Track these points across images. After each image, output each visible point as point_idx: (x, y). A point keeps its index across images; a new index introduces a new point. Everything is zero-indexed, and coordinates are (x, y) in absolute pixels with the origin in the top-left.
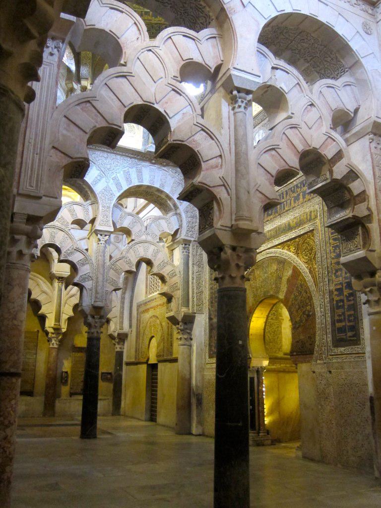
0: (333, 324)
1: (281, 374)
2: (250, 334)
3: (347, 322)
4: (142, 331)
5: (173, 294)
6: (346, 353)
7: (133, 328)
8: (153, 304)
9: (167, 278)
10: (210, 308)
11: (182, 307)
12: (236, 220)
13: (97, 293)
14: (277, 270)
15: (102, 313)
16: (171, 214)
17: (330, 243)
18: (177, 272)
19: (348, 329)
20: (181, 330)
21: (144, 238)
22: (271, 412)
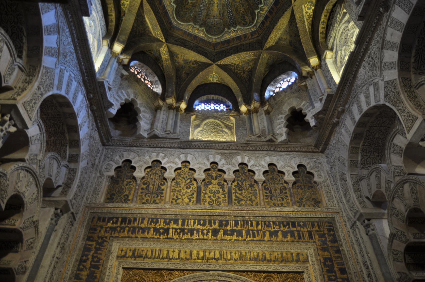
21: (35, 167)
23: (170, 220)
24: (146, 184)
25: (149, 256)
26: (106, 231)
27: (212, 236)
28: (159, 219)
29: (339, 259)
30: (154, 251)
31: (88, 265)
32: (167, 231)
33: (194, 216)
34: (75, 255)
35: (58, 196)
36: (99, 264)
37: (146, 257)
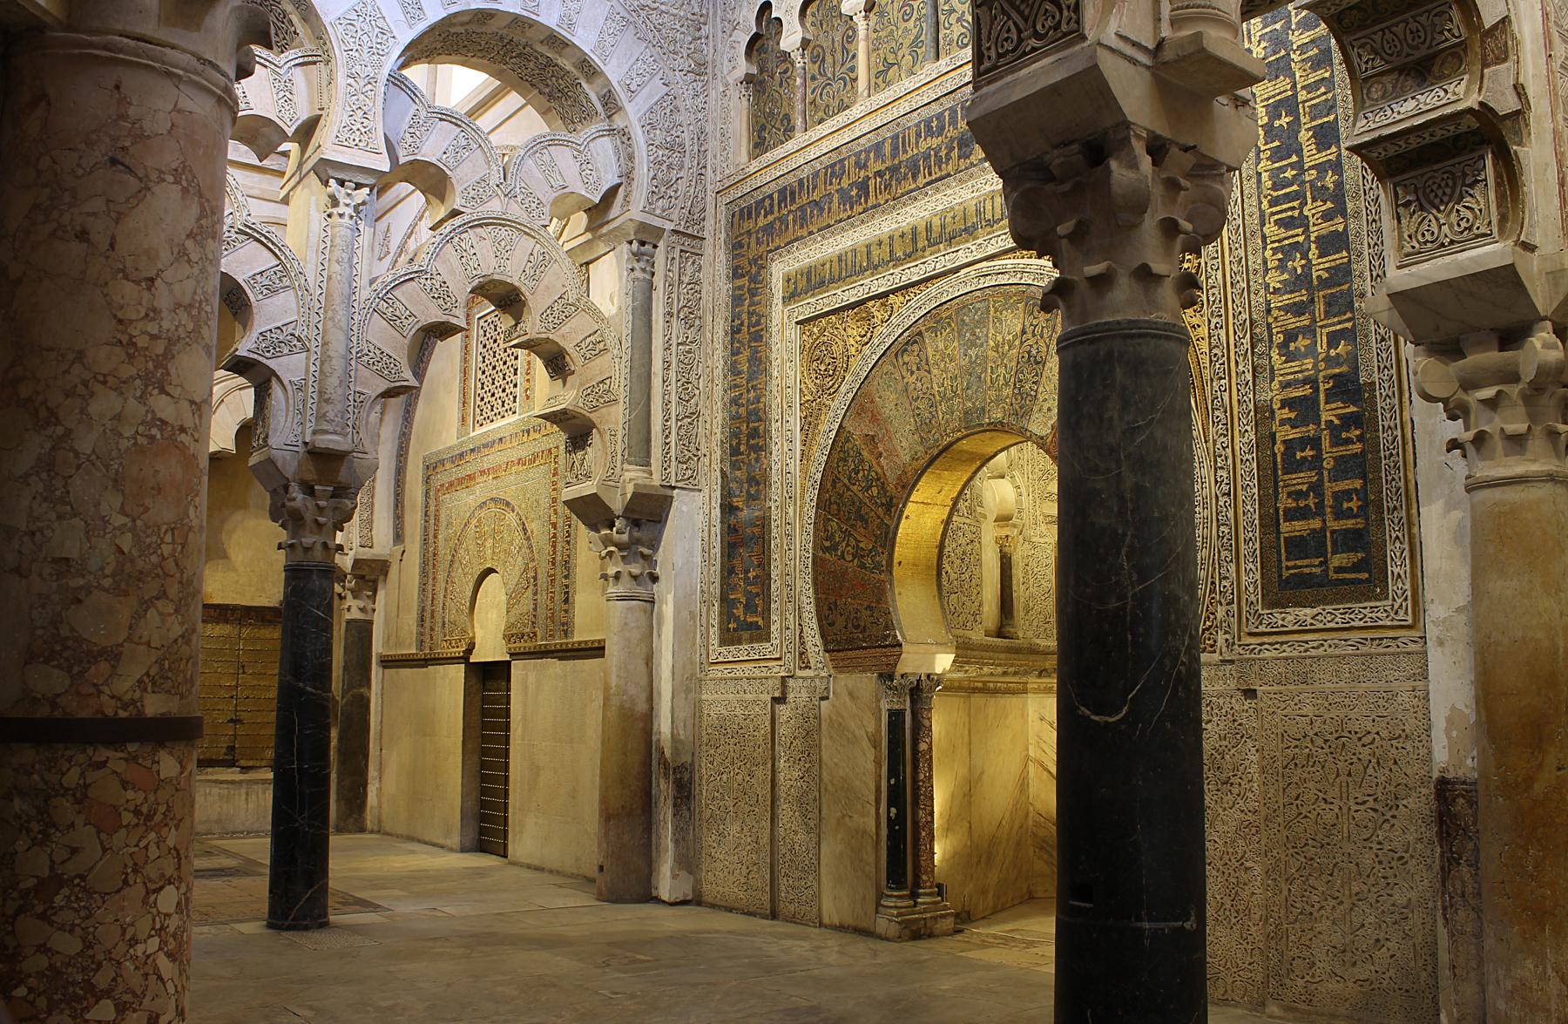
0: (1269, 522)
1: (977, 699)
2: (896, 561)
3: (1329, 517)
4: (444, 552)
5: (592, 416)
6: (1321, 626)
7: (407, 540)
8: (493, 458)
9: (575, 359)
10: (727, 469)
11: (626, 466)
12: (1175, 23)
13: (324, 398)
14: (1024, 332)
15: (343, 475)
16: (592, 129)
17: (1264, 238)
18: (611, 342)
19: (1334, 543)
20: (621, 547)
21: (495, 207)
22: (948, 829)
23: (867, 151)
24: (818, 56)
25: (837, 277)
26: (758, 243)
27: (959, 158)
28: (845, 159)
29: (1323, 90)
30: (844, 258)
31: (744, 335)
32: (863, 187)
33: (915, 113)
34: (722, 322)
35: (619, 213)
36: (759, 328)
37: (832, 281)
